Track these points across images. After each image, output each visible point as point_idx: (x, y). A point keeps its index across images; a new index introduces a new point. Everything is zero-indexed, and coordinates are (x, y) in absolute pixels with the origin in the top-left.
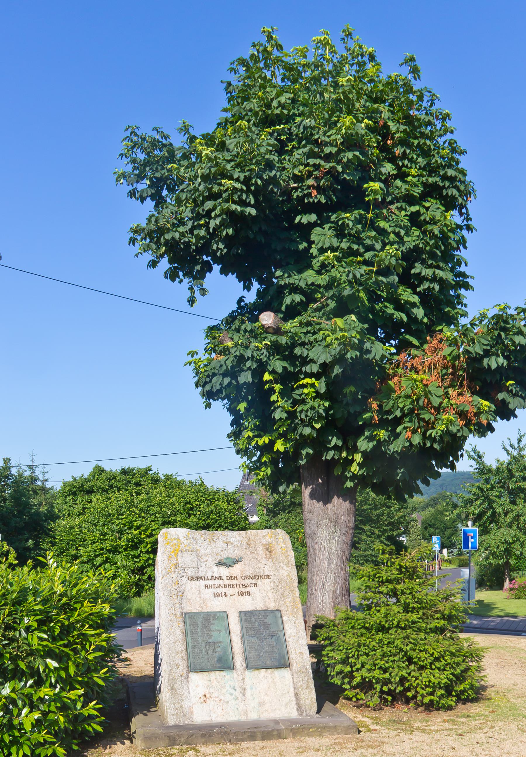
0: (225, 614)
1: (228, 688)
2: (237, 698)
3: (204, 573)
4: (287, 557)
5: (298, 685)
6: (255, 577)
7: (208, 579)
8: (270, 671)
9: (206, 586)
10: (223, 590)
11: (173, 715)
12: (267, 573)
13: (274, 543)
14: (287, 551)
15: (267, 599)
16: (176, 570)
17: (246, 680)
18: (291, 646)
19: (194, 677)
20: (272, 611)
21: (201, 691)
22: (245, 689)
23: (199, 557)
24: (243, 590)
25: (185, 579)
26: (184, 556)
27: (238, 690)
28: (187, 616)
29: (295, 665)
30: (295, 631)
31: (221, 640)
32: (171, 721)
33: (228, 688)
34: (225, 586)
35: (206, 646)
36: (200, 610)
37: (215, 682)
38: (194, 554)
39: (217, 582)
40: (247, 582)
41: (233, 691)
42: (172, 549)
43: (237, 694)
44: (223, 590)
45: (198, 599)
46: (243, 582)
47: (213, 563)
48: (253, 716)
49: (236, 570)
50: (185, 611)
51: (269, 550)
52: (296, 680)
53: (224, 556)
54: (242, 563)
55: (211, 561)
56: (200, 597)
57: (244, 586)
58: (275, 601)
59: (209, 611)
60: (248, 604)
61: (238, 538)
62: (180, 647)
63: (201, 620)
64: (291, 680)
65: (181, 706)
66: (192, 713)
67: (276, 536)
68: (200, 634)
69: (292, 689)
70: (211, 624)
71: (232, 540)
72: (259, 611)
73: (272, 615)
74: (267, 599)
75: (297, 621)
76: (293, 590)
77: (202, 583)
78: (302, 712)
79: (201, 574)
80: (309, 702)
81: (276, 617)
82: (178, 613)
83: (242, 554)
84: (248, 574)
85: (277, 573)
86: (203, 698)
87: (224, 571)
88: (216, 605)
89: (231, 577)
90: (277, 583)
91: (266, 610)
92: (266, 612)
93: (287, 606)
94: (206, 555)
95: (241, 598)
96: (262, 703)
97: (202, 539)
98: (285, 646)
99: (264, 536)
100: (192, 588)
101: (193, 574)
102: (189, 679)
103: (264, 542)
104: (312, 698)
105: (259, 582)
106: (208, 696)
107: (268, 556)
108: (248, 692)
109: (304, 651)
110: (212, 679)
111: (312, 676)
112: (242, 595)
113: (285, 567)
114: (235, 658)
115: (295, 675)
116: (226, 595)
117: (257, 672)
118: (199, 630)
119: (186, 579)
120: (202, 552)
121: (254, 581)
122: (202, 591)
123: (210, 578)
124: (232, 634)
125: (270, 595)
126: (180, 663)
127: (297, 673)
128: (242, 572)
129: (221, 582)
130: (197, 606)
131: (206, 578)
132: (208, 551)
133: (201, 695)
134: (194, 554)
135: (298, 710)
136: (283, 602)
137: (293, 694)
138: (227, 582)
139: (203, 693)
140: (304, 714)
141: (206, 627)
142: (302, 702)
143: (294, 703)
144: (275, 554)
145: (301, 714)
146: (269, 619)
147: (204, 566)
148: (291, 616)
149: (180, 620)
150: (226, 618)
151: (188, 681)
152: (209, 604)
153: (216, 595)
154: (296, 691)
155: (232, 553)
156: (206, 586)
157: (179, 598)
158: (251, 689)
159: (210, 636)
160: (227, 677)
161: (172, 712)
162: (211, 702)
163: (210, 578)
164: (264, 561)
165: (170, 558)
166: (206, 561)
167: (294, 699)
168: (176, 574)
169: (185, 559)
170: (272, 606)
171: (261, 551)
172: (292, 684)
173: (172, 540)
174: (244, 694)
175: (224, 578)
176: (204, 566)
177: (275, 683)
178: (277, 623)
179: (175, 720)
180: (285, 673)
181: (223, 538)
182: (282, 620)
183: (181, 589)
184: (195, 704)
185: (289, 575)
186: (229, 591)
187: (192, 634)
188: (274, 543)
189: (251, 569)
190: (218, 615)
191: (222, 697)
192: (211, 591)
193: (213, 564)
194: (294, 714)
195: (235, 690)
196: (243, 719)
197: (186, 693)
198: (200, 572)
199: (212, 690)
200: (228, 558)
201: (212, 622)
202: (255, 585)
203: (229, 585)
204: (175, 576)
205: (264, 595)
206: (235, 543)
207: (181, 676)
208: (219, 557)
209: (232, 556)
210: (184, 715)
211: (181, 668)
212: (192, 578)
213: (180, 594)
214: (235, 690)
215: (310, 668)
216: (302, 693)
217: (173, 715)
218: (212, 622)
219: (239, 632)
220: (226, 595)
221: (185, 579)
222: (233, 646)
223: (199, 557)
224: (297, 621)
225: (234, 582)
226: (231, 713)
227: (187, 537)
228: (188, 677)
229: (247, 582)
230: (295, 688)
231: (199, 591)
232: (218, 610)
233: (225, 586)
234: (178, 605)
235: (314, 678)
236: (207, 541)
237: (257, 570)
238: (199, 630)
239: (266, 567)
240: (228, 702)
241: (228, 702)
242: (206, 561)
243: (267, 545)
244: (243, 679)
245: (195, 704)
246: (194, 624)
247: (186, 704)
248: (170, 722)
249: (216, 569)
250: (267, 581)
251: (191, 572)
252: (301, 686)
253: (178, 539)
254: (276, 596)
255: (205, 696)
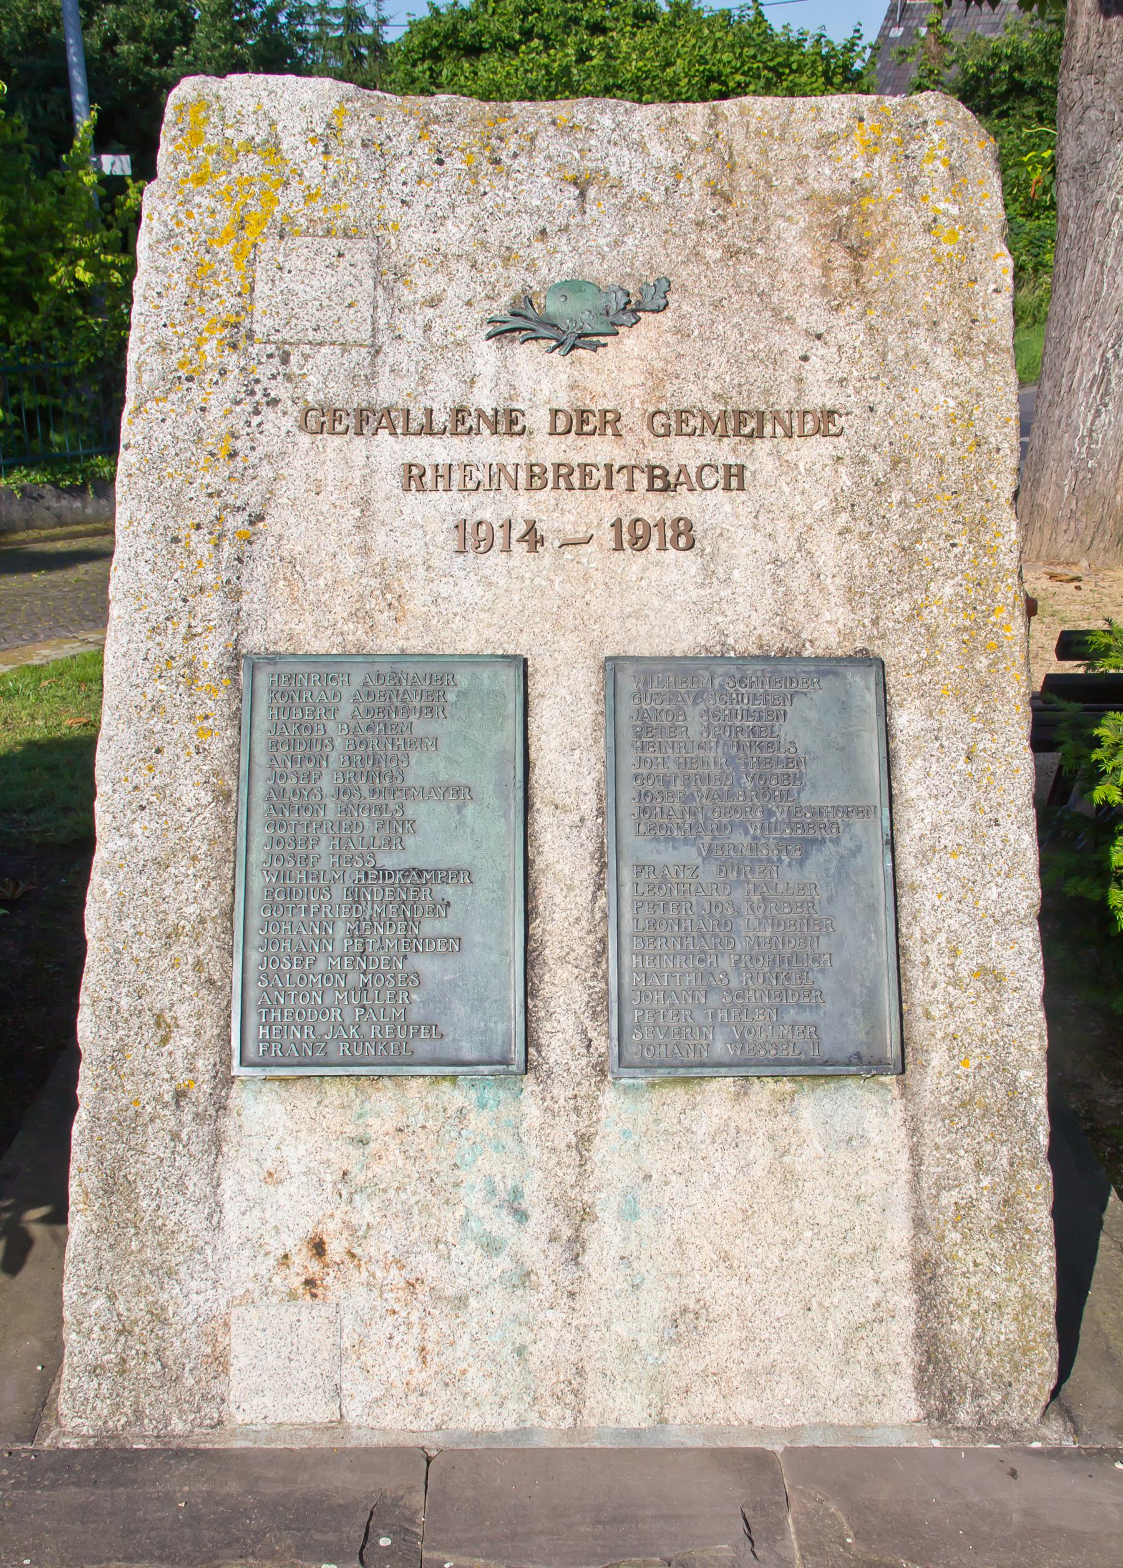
0: (509, 678)
1: (472, 1198)
2: (525, 1278)
3: (407, 384)
4: (963, 286)
5: (948, 1198)
6: (743, 423)
7: (427, 429)
8: (764, 1092)
9: (412, 477)
10: (522, 506)
11: (95, 1370)
12: (820, 396)
13: (889, 189)
14: (967, 250)
15: (800, 581)
16: (232, 360)
17: (600, 1150)
18: (927, 920)
19: (263, 1111)
20: (830, 666)
21: (295, 1211)
22: (586, 1214)
23: (389, 275)
24: (650, 508)
25: (279, 424)
26: (295, 262)
27: (540, 1218)
28: (263, 680)
29: (938, 1058)
30: (963, 813)
31: (464, 861)
32: (81, 1414)
33: (472, 1198)
34: (535, 477)
35: (356, 895)
36: (355, 634)
37: (395, 1155)
38: (360, 252)
39: (487, 449)
40: (685, 452)
41: (503, 1225)
42: (226, 215)
43: (531, 1244)
44: (522, 506)
45: (351, 563)
46: (654, 454)
47: (477, 315)
48: (620, 1409)
49: (620, 370)
50: (255, 641)
51: (850, 234)
52: (932, 1168)
53: (558, 263)
54: (666, 319)
55: (466, 302)
56: (365, 550)
57: (663, 481)
58: (852, 596)
59: (415, 645)
60: (668, 608)
61: (657, 150)
62: (192, 896)
63: (346, 709)
64: (903, 1162)
65: (158, 1316)
66: (220, 1362)
67: (903, 142)
68: (332, 812)
69: (899, 1233)
70: (419, 743)
71: (620, 162)
72: (745, 658)
73: (823, 690)
74: (800, 581)
75: (986, 742)
76: (979, 524)
77: (390, 450)
78: (948, 1399)
79: (386, 393)
80: (1004, 1328)
81: (845, 707)
82: (211, 653)
83: (667, 260)
84: (693, 395)
85: (879, 395)
86: (303, 1262)
87: (540, 377)
88: (465, 609)
89: (583, 415)
90: (879, 465)
91: (784, 656)
92: (782, 670)
93: (931, 633)
94: (439, 260)
95: (633, 564)
96: (686, 1323)
97: (423, 150)
98: (885, 919)
99: (826, 141)
100: (316, 484)
101: (340, 393)
102: (228, 1124)
103: (824, 178)
104: (1028, 1300)
105: (761, 457)
106: (335, 1249)
107: (840, 275)
108: (606, 1239)
109: (1009, 963)
110: (376, 1126)
111: (1044, 1140)
112: (640, 543)
113: (943, 361)
114: (546, 990)
115: (932, 1127)
116: (533, 538)
117: (678, 1095)
118: (327, 784)
119: (288, 423)
120: (415, 239)
121: (724, 452)
122: (381, 507)
123: (441, 418)
124: (543, 817)
125: (827, 548)
126: (182, 1011)
127: (947, 1116)
128: (657, 379)
129: (511, 451)
130: (341, 611)
131: (418, 418)
132: (453, 233)
133: (293, 1242)
134: (360, 252)
135: (922, 1384)
136: (903, 606)
137: (904, 1267)
138: (551, 451)
139: (307, 1227)
140: (965, 1415)
141: (377, 771)
142: (961, 1327)
143: (905, 1326)
144: (886, 263)
145: (940, 1417)
146: (802, 725)
147: (412, 332)
148: (950, 707)
149: (215, 706)
150: (514, 706)
151: (217, 1142)
152: (418, 604)
153: (472, 538)
154: (927, 1242)
155: (607, 249)
156: (412, 477)
157: (227, 550)
158: (630, 1213)
159: (396, 830)
160: (478, 1121)
161: (94, 1349)
162: (350, 1293)
163: (441, 418)
164: (811, 313)
165: (200, 279)
166: (433, 302)
167: (905, 1301)
168: (232, 385)
169: (303, 284)
170: (829, 628)
171: (795, 242)
172: (901, 1192)
173: (226, 155)
174: (575, 1249)
175: (538, 419)
176: (412, 332)
177: (789, 1178)
178: (847, 753)
179: (103, 1407)
180: (869, 1112)
181: (560, 146)
182: (888, 734)
183: (250, 493)
184: (247, 1300)
185: (963, 416)
186: (561, 512)
187: (280, 805)
188: (889, 189)
189: (719, 363)
190: (463, 678)
191: (426, 1263)
192: (440, 506)
193: (469, 325)
194: (896, 1413)
195: (521, 1216)
196: (550, 1425)
197: (195, 1221)
198: (385, 377)
199: (365, 1212)
200: (573, 287)
201: (421, 727)
202: (735, 477)
203: (566, 476)
204: (217, 400)
205: (786, 545)
206: (636, 185)
207: (180, 1095)
208: (518, 277)
209: (605, 270)
210: (169, 1377)
211: (182, 1041)
212: (323, 420)
213: (235, 522)
214: (521, 1216)
215: (1041, 1084)
216: (966, 1258)
217: (95, 1370)
218: (421, 727)
219: (589, 805)
220: (533, 538)
221: (279, 424)
222: (541, 903)
223: (389, 275)
224: (986, 742)
225: (600, 450)
226: (477, 1383)
227: (328, 139)
228: (222, 1108)
229: (685, 452)
230: (919, 1223)
231: (364, 503)
232: (469, 645)
233: (535, 477)
234: (212, 604)
235: (1054, 1155)
236: (454, 163)
237: (755, 372)
238: (327, 784)
239: (819, 350)
240: (461, 1301)
241: (461, 1301)
242: (433, 302)
243: (839, 200)
244: (584, 1140)
245: (247, 1300)
246: (300, 745)
247: (189, 1299)
248: (69, 1423)
249: (486, 356)
250: (814, 451)
251: (322, 378)
252: (964, 1211)
253: (272, 148)
254: (861, 560)
255: (318, 1248)
